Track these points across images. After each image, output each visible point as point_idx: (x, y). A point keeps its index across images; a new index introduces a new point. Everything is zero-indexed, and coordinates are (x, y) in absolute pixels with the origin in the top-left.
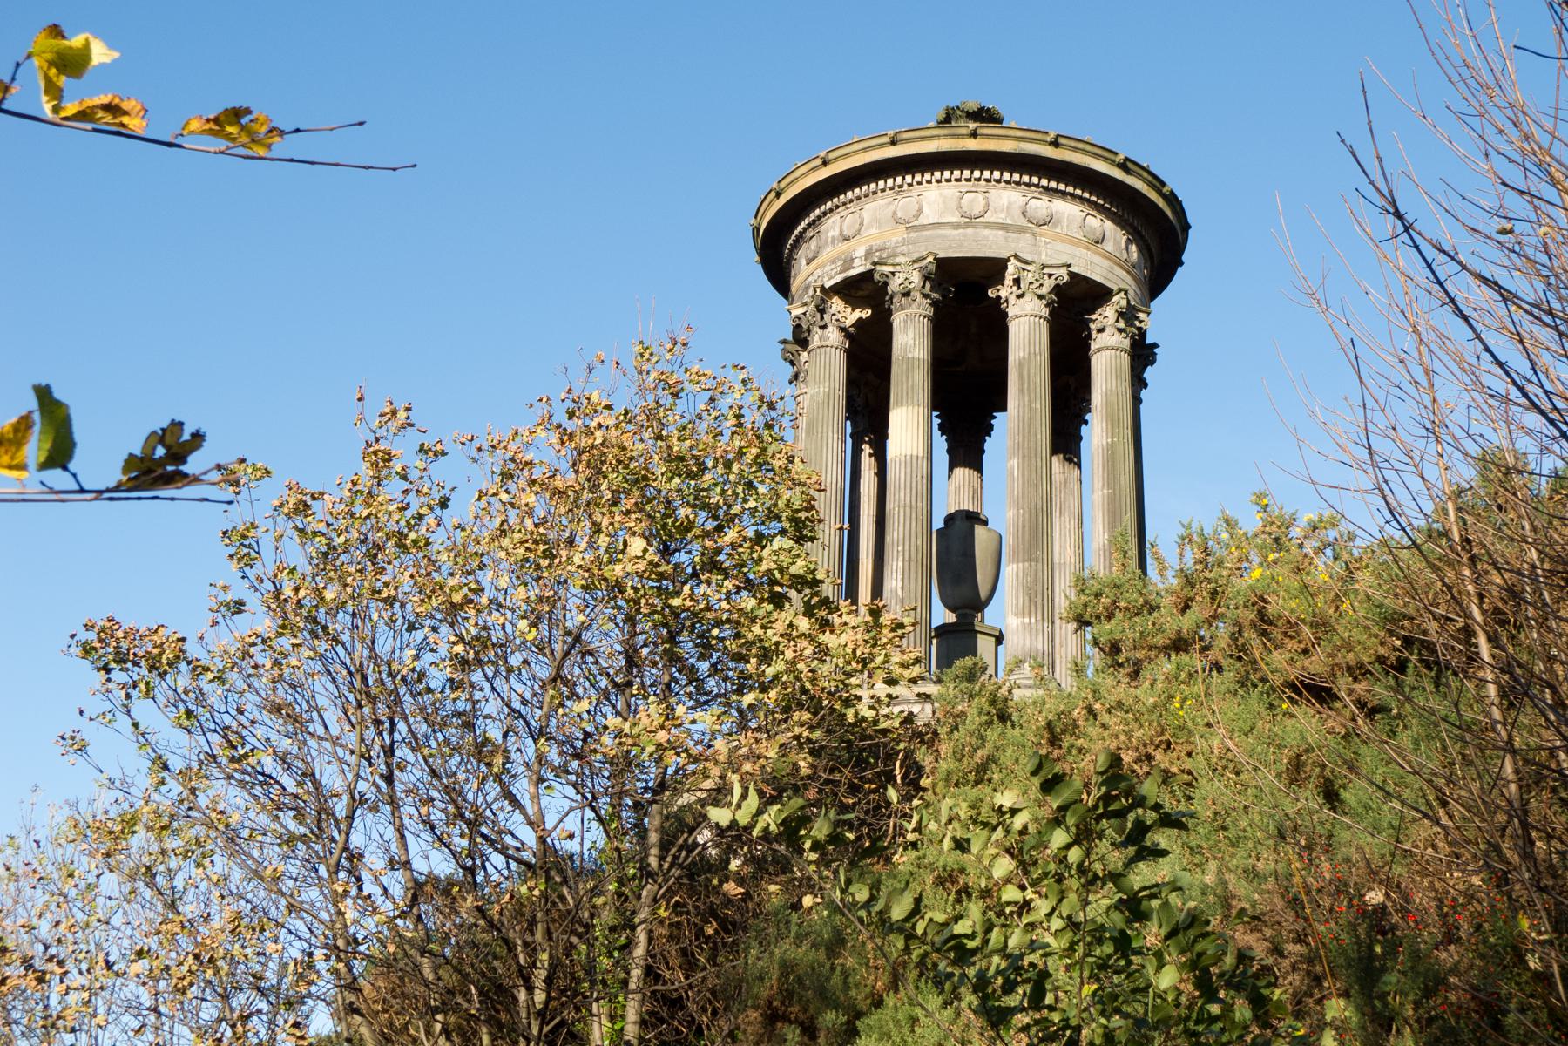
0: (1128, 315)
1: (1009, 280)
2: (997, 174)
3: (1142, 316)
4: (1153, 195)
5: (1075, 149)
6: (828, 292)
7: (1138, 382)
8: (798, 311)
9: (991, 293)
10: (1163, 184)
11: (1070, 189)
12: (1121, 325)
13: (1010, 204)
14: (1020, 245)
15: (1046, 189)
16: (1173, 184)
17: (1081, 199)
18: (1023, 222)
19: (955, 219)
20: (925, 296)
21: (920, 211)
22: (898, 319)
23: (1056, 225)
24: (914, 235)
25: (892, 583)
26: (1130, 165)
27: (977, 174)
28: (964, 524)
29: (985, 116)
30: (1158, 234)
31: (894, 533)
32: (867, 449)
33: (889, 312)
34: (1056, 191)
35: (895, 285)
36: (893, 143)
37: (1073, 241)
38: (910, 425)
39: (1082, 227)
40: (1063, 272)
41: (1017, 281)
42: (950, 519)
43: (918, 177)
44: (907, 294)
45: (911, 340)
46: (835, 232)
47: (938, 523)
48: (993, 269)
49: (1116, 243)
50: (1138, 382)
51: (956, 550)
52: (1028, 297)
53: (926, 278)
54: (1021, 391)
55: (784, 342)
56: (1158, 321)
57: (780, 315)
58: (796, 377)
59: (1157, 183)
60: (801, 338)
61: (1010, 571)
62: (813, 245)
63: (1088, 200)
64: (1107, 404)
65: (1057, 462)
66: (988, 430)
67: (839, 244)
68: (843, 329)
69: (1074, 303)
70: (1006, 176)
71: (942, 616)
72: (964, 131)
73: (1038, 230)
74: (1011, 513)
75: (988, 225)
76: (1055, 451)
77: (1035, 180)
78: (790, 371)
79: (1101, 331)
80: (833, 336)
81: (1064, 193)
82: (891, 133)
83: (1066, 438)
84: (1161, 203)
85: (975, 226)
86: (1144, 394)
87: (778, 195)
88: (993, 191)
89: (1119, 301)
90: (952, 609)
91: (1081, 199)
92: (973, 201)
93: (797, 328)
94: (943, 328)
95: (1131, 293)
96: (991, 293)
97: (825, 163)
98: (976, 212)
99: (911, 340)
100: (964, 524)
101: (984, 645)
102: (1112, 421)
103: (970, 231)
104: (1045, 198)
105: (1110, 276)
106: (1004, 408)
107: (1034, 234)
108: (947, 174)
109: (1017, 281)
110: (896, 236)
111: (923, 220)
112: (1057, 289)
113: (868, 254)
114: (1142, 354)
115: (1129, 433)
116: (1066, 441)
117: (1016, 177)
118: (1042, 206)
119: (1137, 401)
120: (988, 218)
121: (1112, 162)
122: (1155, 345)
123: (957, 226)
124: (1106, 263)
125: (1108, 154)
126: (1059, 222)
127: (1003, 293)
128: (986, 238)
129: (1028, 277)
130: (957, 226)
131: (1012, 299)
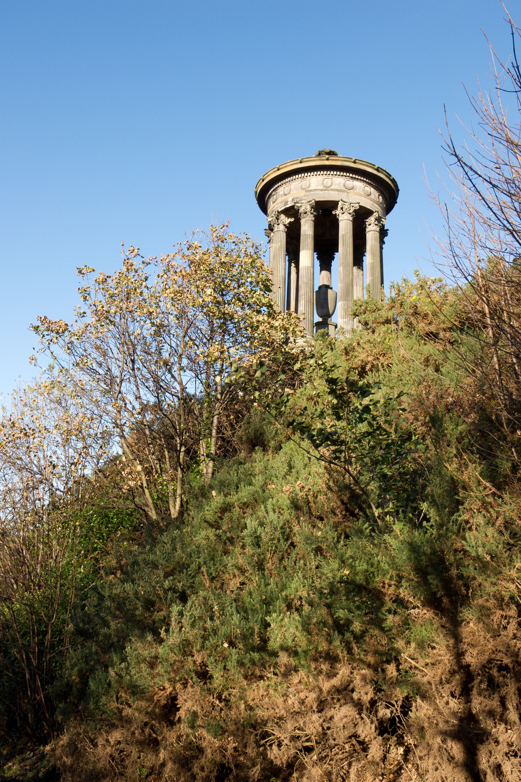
0: (379, 219)
1: (339, 208)
2: (335, 173)
3: (383, 220)
4: (387, 180)
5: (361, 164)
6: (280, 213)
7: (382, 242)
8: (270, 219)
9: (333, 213)
10: (391, 176)
11: (360, 178)
12: (376, 223)
15: (352, 177)
16: (394, 176)
17: (363, 181)
18: (344, 189)
19: (321, 188)
20: (312, 214)
21: (310, 185)
22: (303, 221)
24: (308, 193)
25: (301, 308)
27: (329, 172)
28: (324, 289)
29: (331, 153)
30: (389, 193)
31: (302, 292)
32: (293, 265)
33: (300, 219)
34: (355, 178)
35: (301, 210)
36: (301, 162)
37: (360, 195)
38: (307, 256)
39: (364, 190)
40: (357, 205)
41: (342, 208)
42: (320, 287)
43: (309, 174)
44: (305, 213)
45: (307, 228)
46: (282, 193)
47: (316, 289)
48: (334, 204)
49: (375, 196)
50: (382, 242)
51: (322, 298)
52: (345, 214)
53: (312, 208)
54: (343, 245)
55: (266, 230)
56: (388, 222)
57: (264, 221)
58: (270, 241)
59: (388, 175)
60: (271, 228)
61: (339, 304)
62: (275, 197)
64: (372, 249)
65: (355, 269)
66: (333, 258)
67: (283, 197)
68: (285, 225)
69: (361, 216)
70: (338, 173)
71: (318, 319)
72: (324, 158)
74: (340, 285)
75: (332, 190)
76: (354, 265)
77: (348, 174)
78: (268, 239)
79: (370, 225)
80: (282, 227)
81: (358, 179)
82: (300, 159)
83: (358, 261)
84: (390, 182)
85: (328, 190)
86: (384, 246)
87: (263, 180)
88: (334, 179)
89: (376, 215)
90: (321, 317)
91: (363, 181)
93: (270, 225)
94: (318, 224)
95: (380, 212)
96: (333, 213)
97: (278, 170)
98: (328, 185)
99: (307, 228)
100: (324, 289)
101: (331, 328)
102: (373, 255)
103: (326, 192)
106: (338, 251)
108: (319, 173)
109: (342, 208)
110: (302, 194)
111: (311, 188)
112: (355, 211)
113: (293, 200)
114: (383, 233)
115: (379, 259)
116: (358, 261)
117: (342, 174)
118: (350, 183)
119: (381, 248)
120: (333, 187)
121: (373, 168)
122: (388, 230)
123: (322, 190)
124: (371, 202)
125: (372, 166)
126: (356, 188)
127: (337, 212)
129: (345, 207)
130: (322, 190)
131: (340, 214)
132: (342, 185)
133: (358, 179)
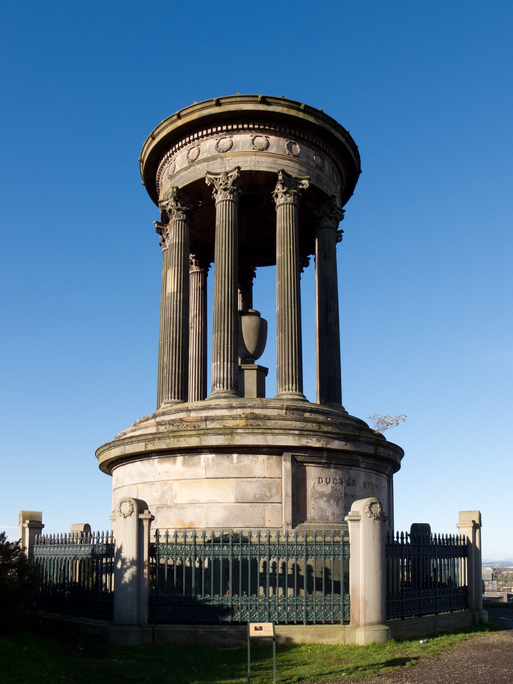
4: (293, 113)
5: (231, 103)
10: (300, 104)
13: (210, 146)
14: (216, 167)
15: (227, 131)
16: (305, 101)
18: (216, 153)
23: (235, 149)
26: (268, 100)
34: (233, 130)
37: (245, 154)
49: (278, 146)
59: (294, 105)
63: (254, 129)
73: (222, 155)
84: (301, 115)
92: (194, 152)
103: (192, 168)
104: (228, 136)
105: (274, 166)
107: (222, 158)
112: (234, 183)
124: (270, 159)
126: (237, 146)
128: (199, 169)
132: (214, 149)
133: (238, 130)
